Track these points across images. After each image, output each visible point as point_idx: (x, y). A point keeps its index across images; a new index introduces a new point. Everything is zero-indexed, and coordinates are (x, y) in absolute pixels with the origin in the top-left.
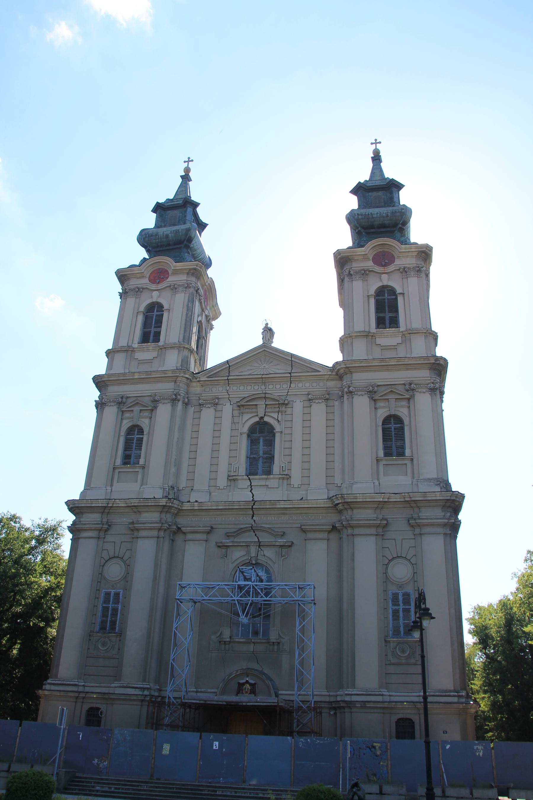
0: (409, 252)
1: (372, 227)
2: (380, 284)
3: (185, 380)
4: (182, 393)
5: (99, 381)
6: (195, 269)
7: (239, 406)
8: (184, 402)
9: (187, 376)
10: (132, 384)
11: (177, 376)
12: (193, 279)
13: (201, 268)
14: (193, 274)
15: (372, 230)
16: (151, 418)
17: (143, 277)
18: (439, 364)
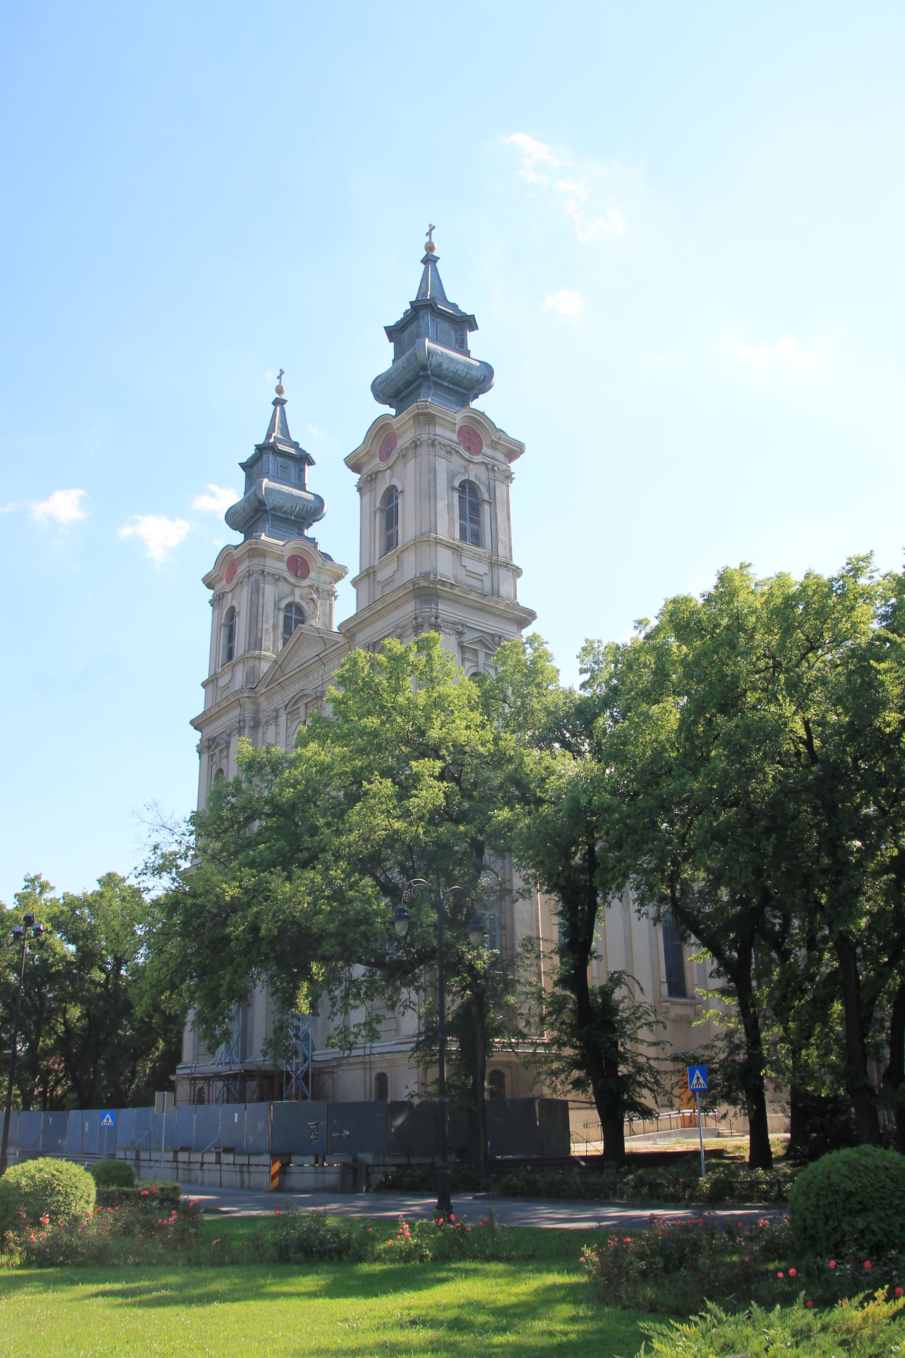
0: (404, 424)
1: (399, 392)
2: (385, 488)
3: (247, 700)
4: (248, 715)
5: (197, 724)
6: (251, 549)
7: (290, 713)
8: (250, 727)
9: (246, 695)
10: (216, 720)
11: (238, 699)
12: (256, 561)
13: (256, 544)
14: (254, 556)
15: (403, 395)
16: (228, 756)
17: (221, 579)
18: (420, 588)
